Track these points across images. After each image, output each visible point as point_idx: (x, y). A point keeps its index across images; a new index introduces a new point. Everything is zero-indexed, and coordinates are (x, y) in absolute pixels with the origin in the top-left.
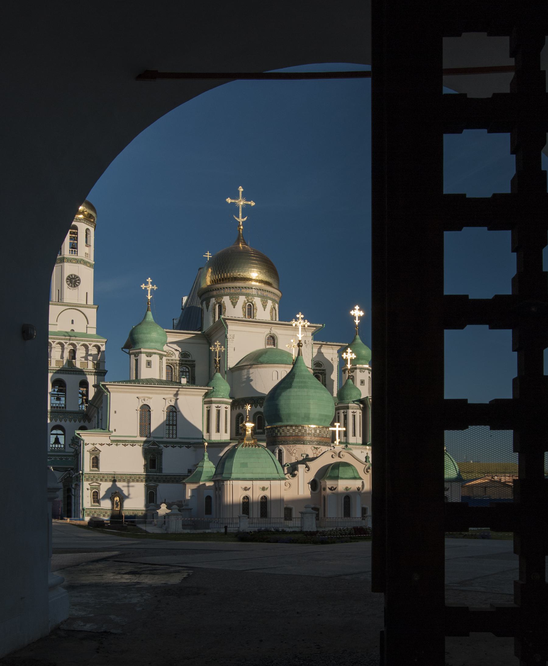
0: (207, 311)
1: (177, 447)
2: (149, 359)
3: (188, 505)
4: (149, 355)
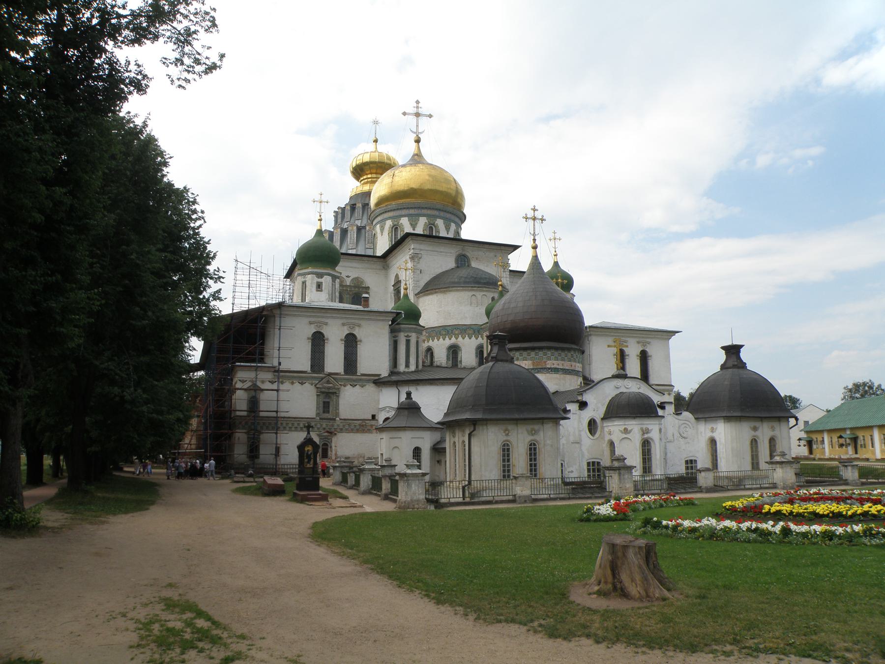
0: (382, 235)
1: (358, 386)
2: (320, 280)
3: (391, 460)
4: (320, 276)
